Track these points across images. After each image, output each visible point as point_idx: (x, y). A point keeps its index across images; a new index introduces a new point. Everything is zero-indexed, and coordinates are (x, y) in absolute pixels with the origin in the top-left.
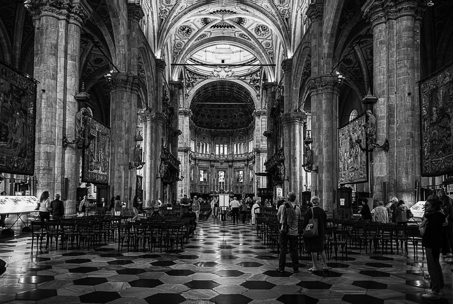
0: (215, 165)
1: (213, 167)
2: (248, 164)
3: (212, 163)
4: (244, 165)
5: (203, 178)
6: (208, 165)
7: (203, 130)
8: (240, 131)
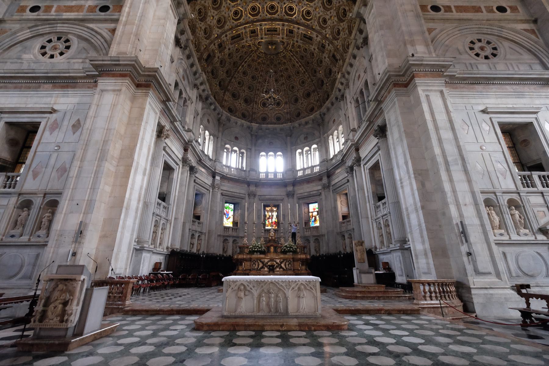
0: (258, 193)
1: (255, 195)
2: (329, 183)
3: (252, 188)
4: (320, 188)
5: (231, 220)
7: (236, 123)
8: (307, 123)
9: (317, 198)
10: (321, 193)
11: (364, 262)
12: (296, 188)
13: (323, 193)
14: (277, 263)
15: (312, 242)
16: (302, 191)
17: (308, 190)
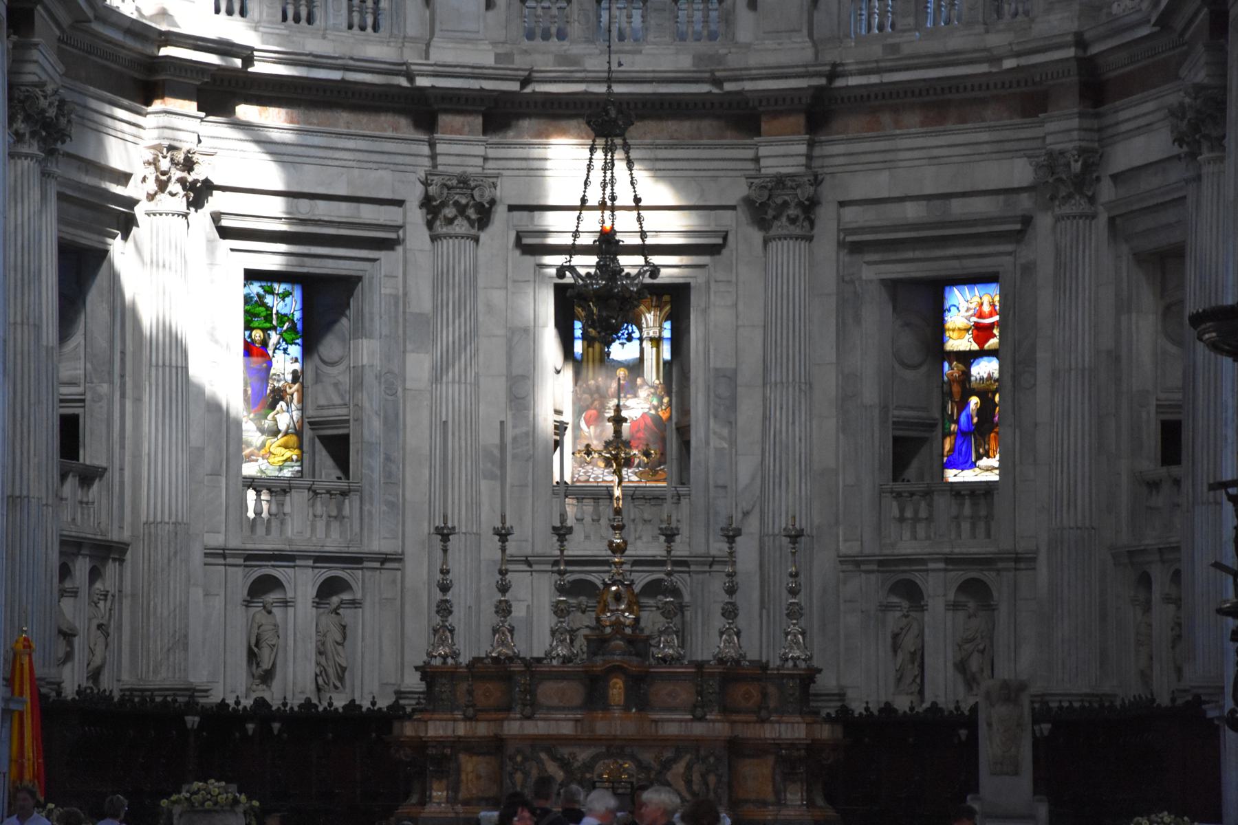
2: (1092, 159)
4: (1020, 172)
6: (380, 182)
9: (999, 256)
10: (1027, 221)
11: (1016, 774)
12: (835, 150)
13: (1044, 221)
14: (641, 766)
15: (936, 604)
16: (878, 184)
17: (931, 181)
